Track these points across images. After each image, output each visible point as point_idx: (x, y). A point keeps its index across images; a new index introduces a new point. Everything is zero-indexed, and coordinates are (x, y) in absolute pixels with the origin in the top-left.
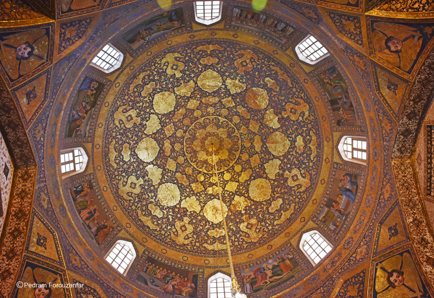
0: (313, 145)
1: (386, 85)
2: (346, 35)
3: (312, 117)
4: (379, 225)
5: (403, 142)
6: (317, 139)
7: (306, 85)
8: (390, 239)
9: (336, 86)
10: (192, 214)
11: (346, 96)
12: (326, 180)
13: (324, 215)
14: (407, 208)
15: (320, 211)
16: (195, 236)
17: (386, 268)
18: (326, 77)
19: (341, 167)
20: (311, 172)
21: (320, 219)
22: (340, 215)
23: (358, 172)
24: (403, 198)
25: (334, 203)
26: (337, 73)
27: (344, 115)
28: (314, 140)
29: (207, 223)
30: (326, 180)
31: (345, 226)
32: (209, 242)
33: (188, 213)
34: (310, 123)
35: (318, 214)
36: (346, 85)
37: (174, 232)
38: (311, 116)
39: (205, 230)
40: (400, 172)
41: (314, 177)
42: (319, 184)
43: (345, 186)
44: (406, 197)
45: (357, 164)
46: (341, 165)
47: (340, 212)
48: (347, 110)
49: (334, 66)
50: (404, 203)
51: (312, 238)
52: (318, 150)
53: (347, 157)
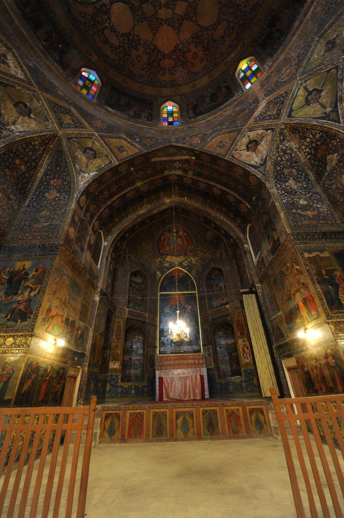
10: (145, 43)
16: (149, 67)
17: (308, 87)
29: (159, 53)
32: (161, 73)
33: (142, 42)
37: (131, 63)
39: (158, 61)
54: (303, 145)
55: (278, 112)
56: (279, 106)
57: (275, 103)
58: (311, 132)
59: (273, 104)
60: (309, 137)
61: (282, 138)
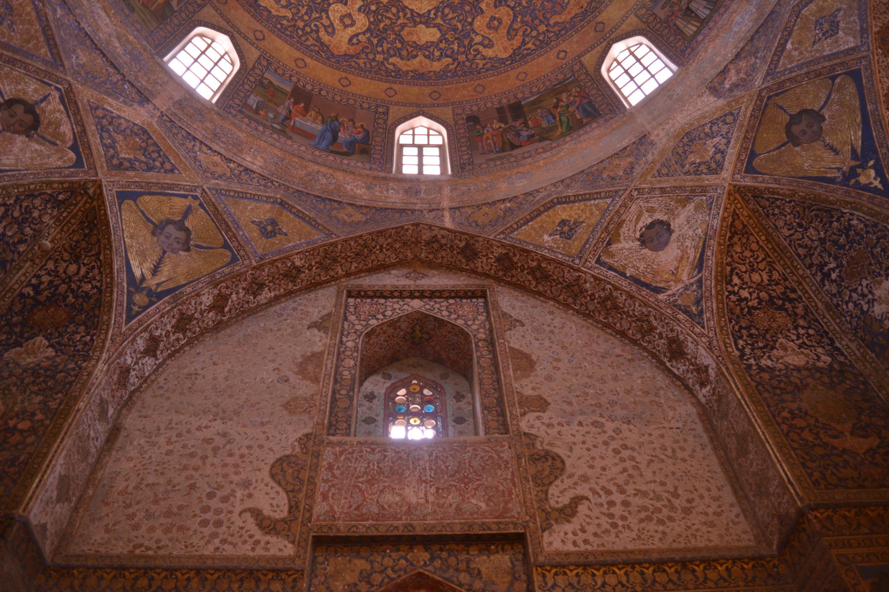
0: (421, 62)
1: (570, 216)
2: (681, 145)
3: (481, 63)
4: (279, 201)
5: (452, 246)
6: (435, 72)
7: (552, 55)
8: (253, 222)
9: (554, 118)
11: (533, 136)
12: (349, 89)
13: (276, 83)
14: (322, 254)
15: (283, 75)
17: (190, 217)
18: (572, 99)
19: (380, 121)
20: (363, 56)
21: (267, 75)
22: (281, 118)
23: (376, 156)
24: (339, 247)
25: (302, 105)
26: (585, 121)
27: (490, 130)
28: (431, 66)
30: (349, 89)
31: (261, 128)
34: (468, 60)
35: (276, 70)
36: (558, 138)
38: (484, 62)
40: (389, 240)
41: (353, 64)
42: (340, 74)
43: (342, 129)
44: (341, 252)
45: (392, 154)
46: (385, 121)
47: (288, 118)
48: (502, 136)
49: (600, 115)
50: (331, 248)
51: (222, 57)
52: (412, 74)
53: (402, 133)
54: (56, 261)
55: (127, 164)
56: (141, 162)
57: (145, 150)
58: (93, 267)
59: (143, 145)
60: (79, 269)
61: (61, 197)
